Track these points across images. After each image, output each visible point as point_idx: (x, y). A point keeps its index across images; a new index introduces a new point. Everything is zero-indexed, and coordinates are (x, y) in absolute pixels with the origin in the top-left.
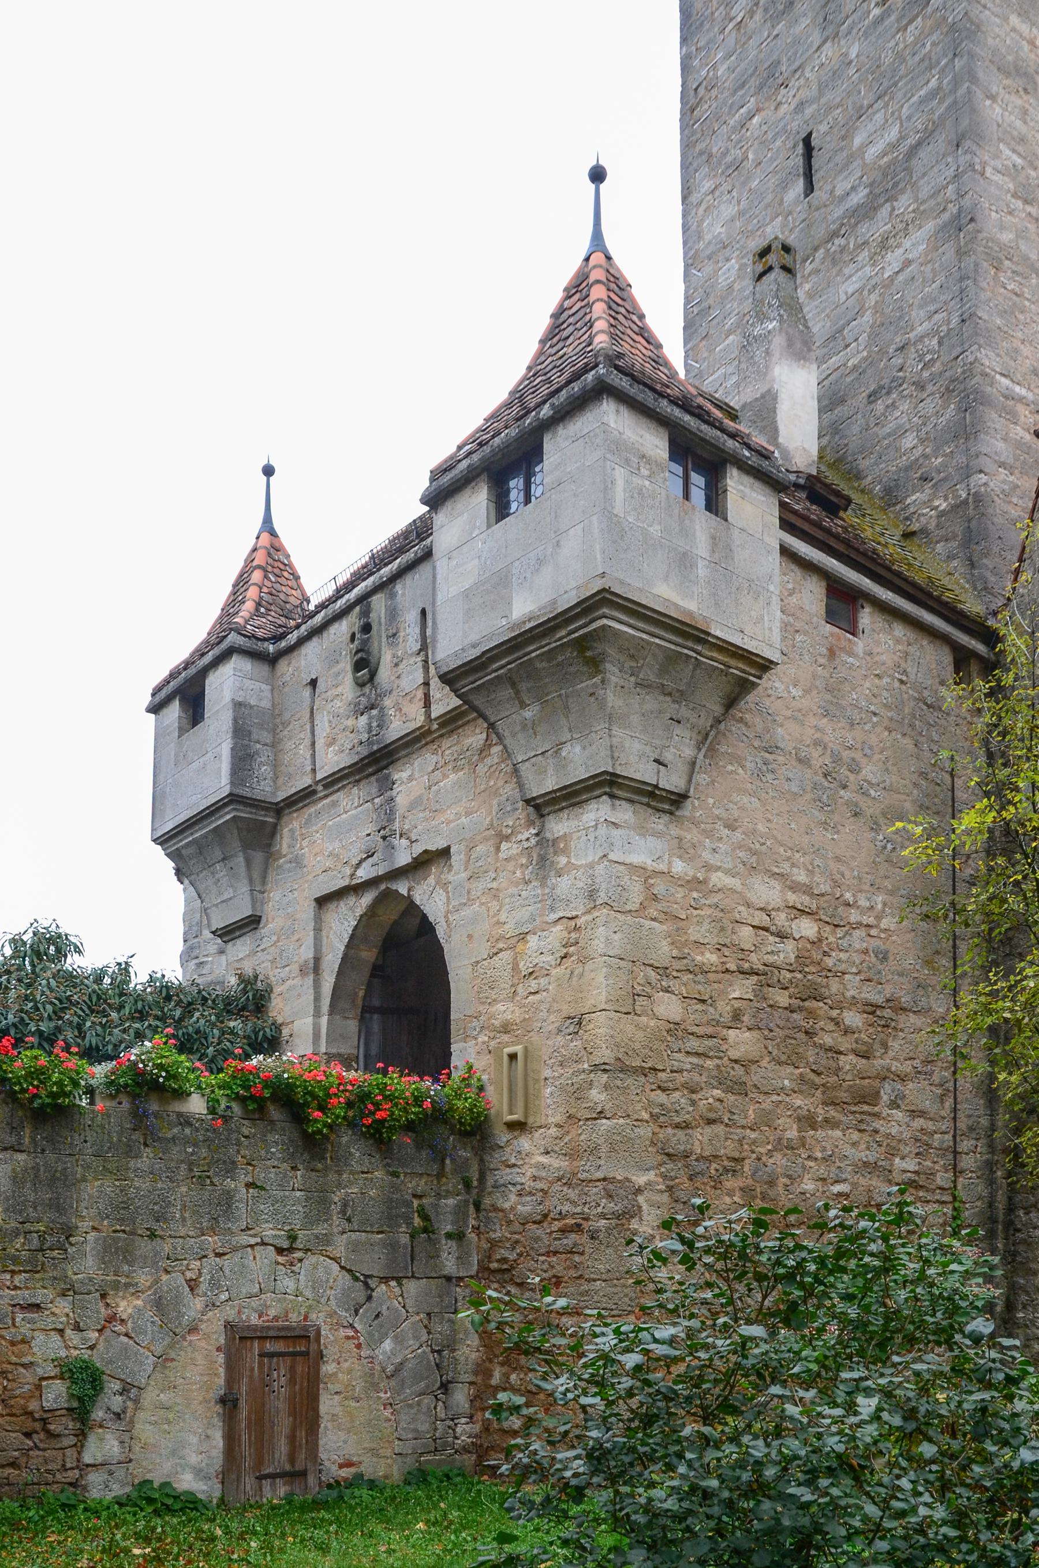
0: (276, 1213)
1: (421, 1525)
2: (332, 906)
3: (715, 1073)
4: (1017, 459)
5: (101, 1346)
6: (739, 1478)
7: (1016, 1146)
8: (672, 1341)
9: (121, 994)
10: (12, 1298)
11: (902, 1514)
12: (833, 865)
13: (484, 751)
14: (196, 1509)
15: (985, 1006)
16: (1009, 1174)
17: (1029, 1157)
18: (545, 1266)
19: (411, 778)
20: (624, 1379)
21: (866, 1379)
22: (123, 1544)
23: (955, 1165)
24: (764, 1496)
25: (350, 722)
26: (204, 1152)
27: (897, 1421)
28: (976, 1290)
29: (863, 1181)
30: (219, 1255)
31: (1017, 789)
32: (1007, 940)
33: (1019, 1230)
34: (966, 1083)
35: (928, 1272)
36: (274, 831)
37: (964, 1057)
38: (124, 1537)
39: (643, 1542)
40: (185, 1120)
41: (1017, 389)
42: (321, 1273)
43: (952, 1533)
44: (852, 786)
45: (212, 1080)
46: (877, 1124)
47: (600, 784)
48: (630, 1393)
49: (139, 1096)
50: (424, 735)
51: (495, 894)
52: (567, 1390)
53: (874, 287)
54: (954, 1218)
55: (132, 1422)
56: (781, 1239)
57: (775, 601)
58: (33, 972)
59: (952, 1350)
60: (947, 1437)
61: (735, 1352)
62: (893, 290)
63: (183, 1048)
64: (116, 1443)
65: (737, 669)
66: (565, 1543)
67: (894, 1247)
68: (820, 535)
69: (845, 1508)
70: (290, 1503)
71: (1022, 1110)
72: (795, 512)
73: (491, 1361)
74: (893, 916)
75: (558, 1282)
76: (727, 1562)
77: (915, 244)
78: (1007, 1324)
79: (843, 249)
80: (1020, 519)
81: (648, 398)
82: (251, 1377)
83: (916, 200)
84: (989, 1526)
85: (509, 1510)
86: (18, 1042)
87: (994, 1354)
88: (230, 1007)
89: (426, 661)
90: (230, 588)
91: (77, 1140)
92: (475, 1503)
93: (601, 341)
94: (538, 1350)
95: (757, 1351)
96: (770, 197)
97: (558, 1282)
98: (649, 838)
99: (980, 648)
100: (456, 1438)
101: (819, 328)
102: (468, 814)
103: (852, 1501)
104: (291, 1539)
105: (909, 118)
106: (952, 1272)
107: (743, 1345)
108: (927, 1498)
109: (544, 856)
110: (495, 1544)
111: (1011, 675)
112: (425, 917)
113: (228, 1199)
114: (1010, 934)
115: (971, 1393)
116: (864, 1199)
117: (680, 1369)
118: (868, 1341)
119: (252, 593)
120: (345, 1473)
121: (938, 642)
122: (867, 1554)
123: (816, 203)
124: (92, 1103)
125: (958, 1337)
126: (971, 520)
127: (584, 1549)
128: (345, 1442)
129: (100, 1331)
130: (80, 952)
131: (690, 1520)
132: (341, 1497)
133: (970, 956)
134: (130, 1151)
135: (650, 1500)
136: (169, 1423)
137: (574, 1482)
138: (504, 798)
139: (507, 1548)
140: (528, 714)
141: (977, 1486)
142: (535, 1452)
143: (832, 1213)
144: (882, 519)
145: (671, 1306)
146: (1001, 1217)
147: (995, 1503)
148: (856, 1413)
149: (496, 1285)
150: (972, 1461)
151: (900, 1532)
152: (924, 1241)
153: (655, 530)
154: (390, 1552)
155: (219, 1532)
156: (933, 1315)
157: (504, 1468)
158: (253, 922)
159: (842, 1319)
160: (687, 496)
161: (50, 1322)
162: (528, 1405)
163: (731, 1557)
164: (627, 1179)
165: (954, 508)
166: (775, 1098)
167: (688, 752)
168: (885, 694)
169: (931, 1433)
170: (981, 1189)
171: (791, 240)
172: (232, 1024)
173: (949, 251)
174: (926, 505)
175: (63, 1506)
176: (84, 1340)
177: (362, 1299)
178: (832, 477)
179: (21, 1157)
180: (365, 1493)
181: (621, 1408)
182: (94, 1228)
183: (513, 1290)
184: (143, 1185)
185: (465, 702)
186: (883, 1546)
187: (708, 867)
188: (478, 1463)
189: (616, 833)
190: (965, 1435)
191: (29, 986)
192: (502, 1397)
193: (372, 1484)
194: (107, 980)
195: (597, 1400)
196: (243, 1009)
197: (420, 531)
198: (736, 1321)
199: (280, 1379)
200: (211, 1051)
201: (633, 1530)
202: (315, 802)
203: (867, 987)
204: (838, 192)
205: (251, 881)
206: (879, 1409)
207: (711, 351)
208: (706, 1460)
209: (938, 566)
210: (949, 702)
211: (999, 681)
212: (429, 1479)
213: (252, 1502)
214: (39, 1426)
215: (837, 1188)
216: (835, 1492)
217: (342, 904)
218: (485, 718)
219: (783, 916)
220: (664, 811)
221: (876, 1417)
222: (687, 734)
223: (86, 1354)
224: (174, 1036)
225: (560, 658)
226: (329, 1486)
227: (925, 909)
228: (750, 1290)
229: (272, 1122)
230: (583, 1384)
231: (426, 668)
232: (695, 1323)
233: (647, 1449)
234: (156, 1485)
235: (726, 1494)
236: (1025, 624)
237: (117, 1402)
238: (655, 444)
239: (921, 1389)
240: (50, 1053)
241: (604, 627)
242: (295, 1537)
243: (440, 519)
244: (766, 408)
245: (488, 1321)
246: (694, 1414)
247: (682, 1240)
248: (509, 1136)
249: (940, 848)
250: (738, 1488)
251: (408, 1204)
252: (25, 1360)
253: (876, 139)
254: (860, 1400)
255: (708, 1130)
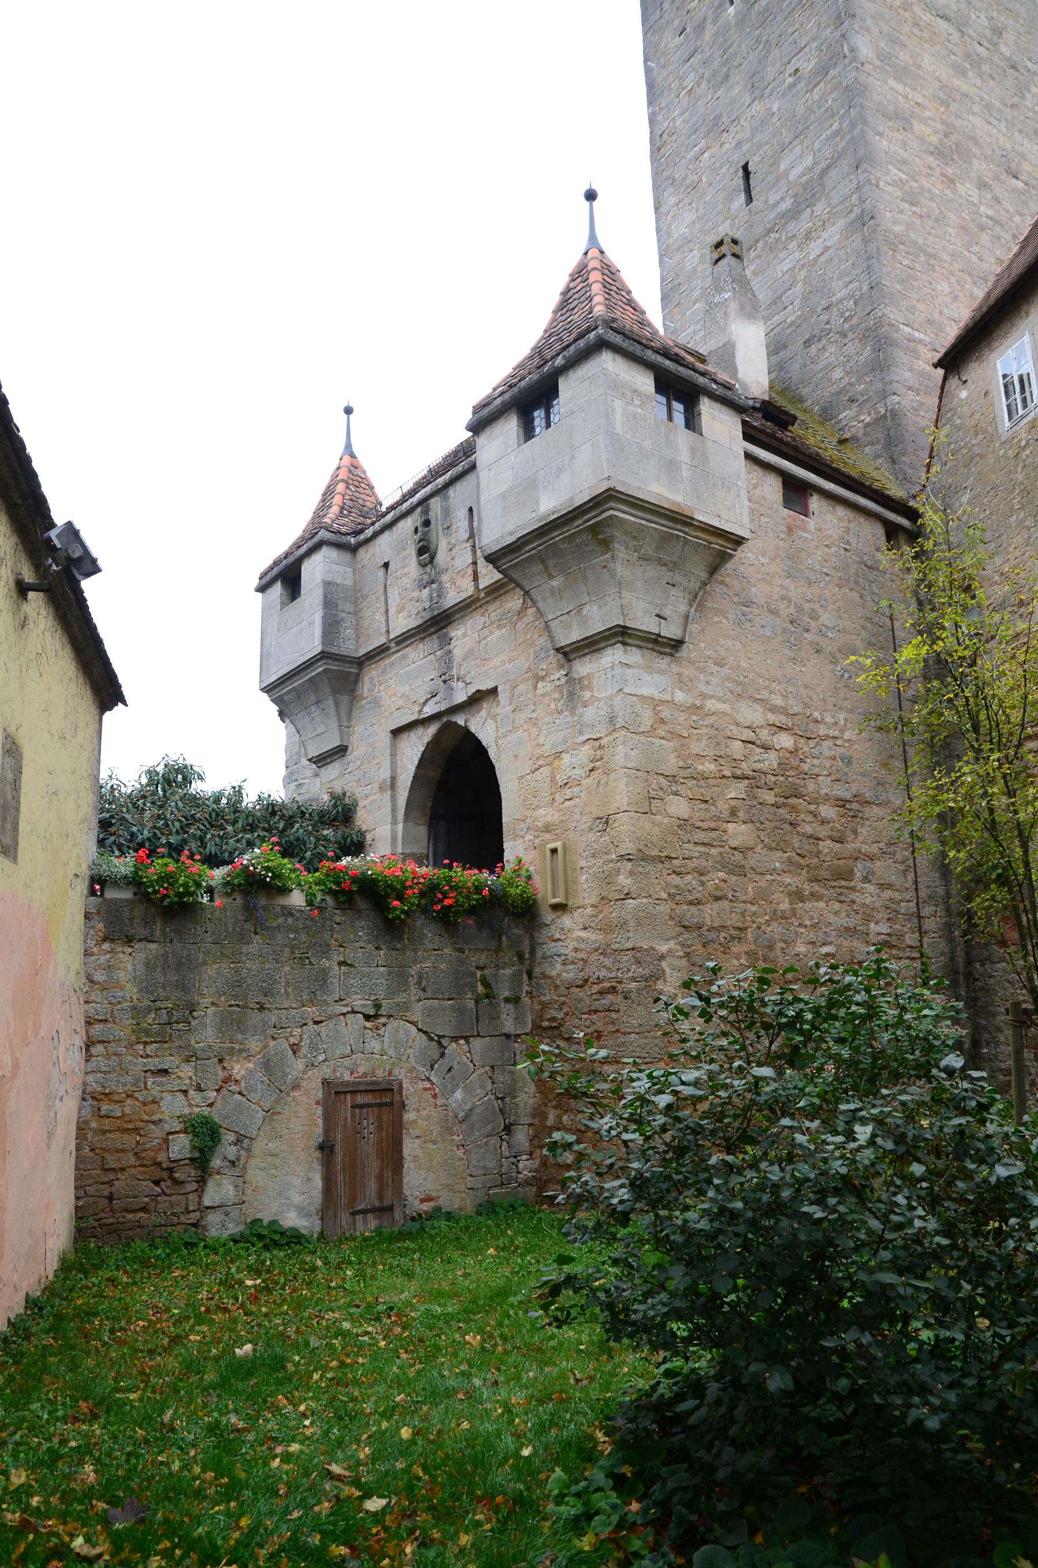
0: (364, 985)
1: (491, 1251)
2: (404, 736)
3: (718, 859)
4: (921, 384)
5: (218, 1104)
6: (760, 1200)
7: (969, 910)
8: (696, 1083)
9: (236, 811)
10: (145, 1065)
11: (899, 1227)
12: (802, 691)
13: (521, 612)
14: (300, 1243)
15: (934, 797)
16: (965, 933)
17: (980, 918)
18: (588, 1023)
19: (464, 635)
20: (658, 1117)
21: (861, 1109)
22: (237, 1276)
23: (920, 928)
24: (782, 1214)
25: (416, 594)
26: (303, 937)
27: (889, 1145)
28: (946, 1031)
29: (845, 943)
30: (317, 1023)
31: (944, 628)
32: (946, 745)
33: (977, 980)
34: (923, 860)
35: (906, 1017)
36: (357, 679)
37: (920, 839)
38: (239, 1271)
39: (682, 1259)
40: (288, 912)
41: (917, 334)
42: (401, 1035)
43: (945, 1242)
44: (813, 630)
45: (310, 878)
46: (853, 896)
47: (615, 635)
48: (664, 1129)
49: (250, 893)
50: (474, 602)
51: (534, 722)
52: (611, 1128)
53: (803, 266)
54: (923, 971)
55: (245, 1168)
56: (781, 994)
57: (743, 494)
58: (165, 796)
59: (930, 1082)
60: (932, 1157)
61: (750, 1091)
62: (817, 268)
63: (287, 852)
64: (231, 1187)
65: (717, 544)
66: (615, 1262)
67: (875, 997)
68: (774, 443)
69: (852, 1223)
70: (379, 1235)
71: (971, 881)
72: (754, 427)
73: (546, 1105)
74: (854, 729)
75: (599, 1035)
76: (754, 1274)
77: (832, 235)
78: (974, 1060)
79: (777, 241)
80: (928, 427)
81: (638, 350)
82: (345, 1126)
83: (830, 205)
84: (976, 1234)
85: (566, 1235)
86: (152, 853)
87: (966, 1085)
88: (324, 818)
89: (474, 546)
90: (320, 497)
91: (200, 931)
92: (537, 1230)
93: (599, 310)
94: (585, 1094)
95: (767, 1089)
96: (720, 207)
97: (599, 1035)
98: (656, 675)
99: (905, 522)
100: (519, 1173)
101: (763, 296)
102: (510, 661)
103: (856, 1217)
104: (381, 1267)
105: (820, 150)
106: (925, 1016)
107: (756, 1084)
108: (920, 1212)
109: (573, 692)
110: (555, 1266)
111: (931, 542)
112: (479, 742)
113: (323, 976)
114: (948, 740)
115: (950, 1119)
116: (847, 958)
117: (704, 1106)
118: (860, 1077)
119: (337, 500)
120: (426, 1207)
121: (872, 520)
122: (873, 1263)
123: (754, 210)
124: (212, 900)
125: (934, 1071)
126: (890, 430)
127: (632, 1267)
128: (425, 1180)
129: (218, 1091)
130: (202, 779)
131: (720, 1238)
132: (423, 1229)
133: (917, 759)
134: (243, 939)
135: (686, 1221)
136: (276, 1168)
137: (620, 1208)
138: (538, 648)
139: (566, 1268)
140: (555, 583)
141: (962, 1200)
142: (586, 1183)
143: (822, 970)
144: (822, 431)
145: (694, 1053)
146: (961, 969)
147: (979, 1213)
148: (855, 1140)
149: (547, 1041)
150: (957, 1178)
151: (900, 1242)
152: (899, 991)
153: (647, 444)
154: (466, 1275)
155: (319, 1263)
156: (913, 1054)
157: (561, 1198)
158: (341, 751)
159: (837, 1058)
160: (670, 418)
161: (176, 1085)
162: (578, 1142)
163: (757, 1270)
164: (652, 948)
165: (877, 421)
166: (769, 877)
167: (683, 608)
168: (834, 559)
169: (919, 1154)
170: (943, 946)
171: (738, 236)
172: (325, 832)
173: (857, 240)
174: (854, 420)
175: (187, 1245)
176: (205, 1098)
177: (437, 1056)
178: (781, 402)
179: (153, 946)
180: (443, 1223)
181: (657, 1142)
182: (213, 1004)
183: (562, 1044)
184: (254, 966)
185: (505, 576)
186: (886, 1255)
187: (703, 696)
188: (539, 1194)
189: (629, 672)
190: (947, 1155)
191: (161, 807)
192: (557, 1136)
193: (449, 1216)
194: (224, 801)
195: (636, 1136)
196: (335, 819)
197: (466, 450)
198: (749, 1064)
199: (369, 1126)
200: (308, 854)
201: (672, 1249)
202: (389, 656)
203: (837, 786)
204: (771, 202)
205: (339, 719)
206: (874, 1136)
207: (683, 315)
208: (731, 1185)
209: (867, 463)
210: (884, 564)
211: (922, 546)
212: (501, 1208)
213: (347, 1235)
214: (166, 1174)
215: (825, 950)
216: (842, 1208)
217: (412, 734)
218: (522, 588)
219: (765, 732)
220: (665, 654)
221: (872, 1142)
222: (681, 594)
223: (206, 1110)
224: (278, 844)
225: (578, 541)
226: (413, 1219)
227: (878, 723)
228: (759, 1037)
229: (359, 911)
230: (624, 1122)
231: (474, 552)
232: (714, 1067)
233: (680, 1177)
234: (265, 1223)
235: (750, 1214)
236: (938, 503)
237: (232, 1152)
238: (646, 382)
239: (907, 1117)
240: (177, 861)
241: (611, 516)
242: (384, 1265)
243: (481, 441)
244: (727, 353)
245: (542, 1071)
246: (718, 1145)
247: (701, 997)
248: (553, 916)
249: (886, 675)
250: (760, 1208)
251: (473, 975)
252: (155, 1118)
253: (797, 165)
254: (857, 1128)
255: (716, 905)
